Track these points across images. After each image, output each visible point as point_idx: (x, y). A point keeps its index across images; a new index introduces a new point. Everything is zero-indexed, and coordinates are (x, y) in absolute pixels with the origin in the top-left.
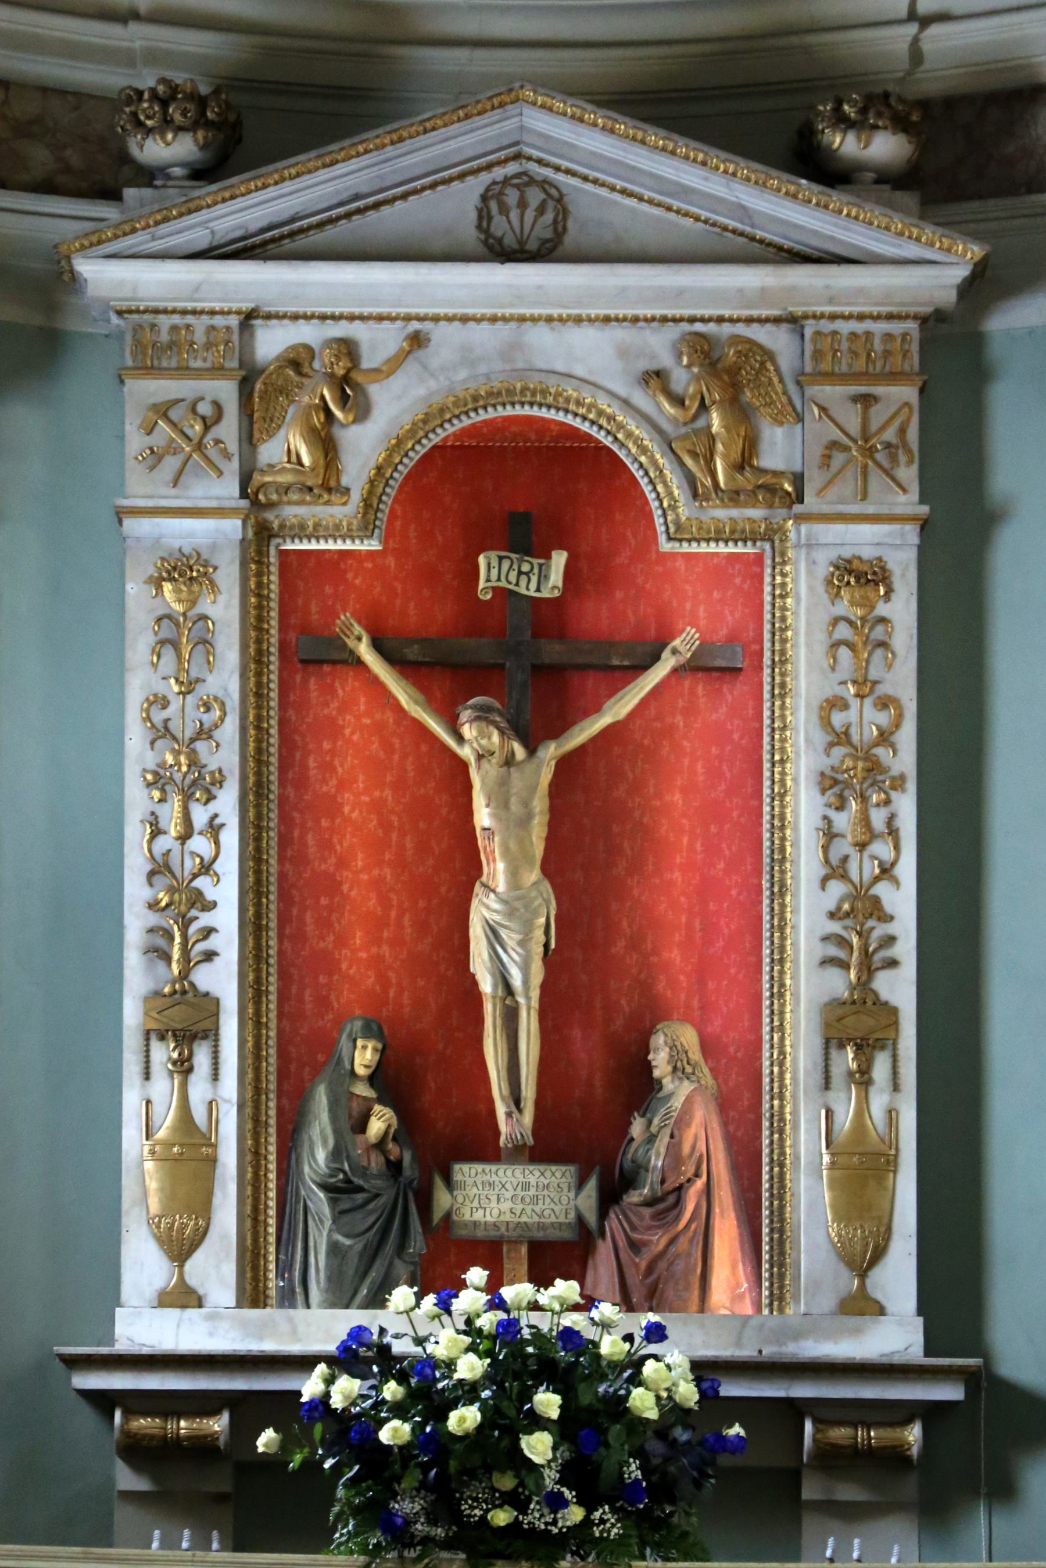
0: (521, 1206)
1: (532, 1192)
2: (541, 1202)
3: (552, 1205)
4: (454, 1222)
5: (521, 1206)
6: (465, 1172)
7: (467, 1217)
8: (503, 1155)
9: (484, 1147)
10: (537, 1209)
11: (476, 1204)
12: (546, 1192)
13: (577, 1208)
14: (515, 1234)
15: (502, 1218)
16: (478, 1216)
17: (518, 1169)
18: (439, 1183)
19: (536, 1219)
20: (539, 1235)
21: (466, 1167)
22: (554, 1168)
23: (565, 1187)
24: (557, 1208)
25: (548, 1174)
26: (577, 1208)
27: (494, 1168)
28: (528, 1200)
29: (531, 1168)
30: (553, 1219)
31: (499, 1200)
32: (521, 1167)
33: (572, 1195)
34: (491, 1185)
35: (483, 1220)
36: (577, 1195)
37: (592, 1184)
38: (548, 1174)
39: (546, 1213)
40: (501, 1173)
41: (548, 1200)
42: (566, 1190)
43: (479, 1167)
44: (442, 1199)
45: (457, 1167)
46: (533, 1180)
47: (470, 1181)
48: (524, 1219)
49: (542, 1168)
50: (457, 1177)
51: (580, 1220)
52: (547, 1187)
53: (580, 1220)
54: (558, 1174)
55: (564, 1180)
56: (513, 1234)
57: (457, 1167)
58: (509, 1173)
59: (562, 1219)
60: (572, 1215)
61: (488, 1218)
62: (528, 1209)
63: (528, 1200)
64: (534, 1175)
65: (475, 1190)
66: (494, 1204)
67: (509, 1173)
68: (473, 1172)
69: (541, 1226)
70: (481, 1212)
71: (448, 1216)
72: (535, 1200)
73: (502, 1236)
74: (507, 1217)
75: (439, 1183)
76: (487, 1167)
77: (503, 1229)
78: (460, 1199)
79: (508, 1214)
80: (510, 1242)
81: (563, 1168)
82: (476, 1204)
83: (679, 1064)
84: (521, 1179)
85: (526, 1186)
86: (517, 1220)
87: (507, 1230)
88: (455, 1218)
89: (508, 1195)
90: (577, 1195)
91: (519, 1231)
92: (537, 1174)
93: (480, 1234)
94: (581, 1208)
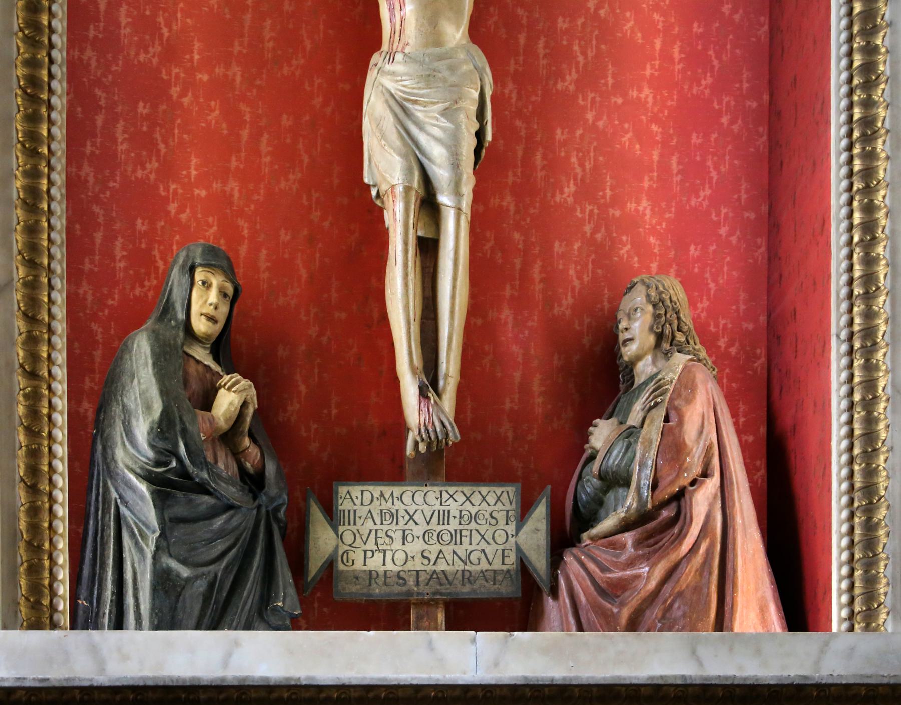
0: (438, 547)
1: (454, 525)
2: (465, 541)
3: (483, 545)
4: (337, 571)
5: (438, 547)
6: (355, 497)
7: (359, 566)
8: (409, 468)
9: (382, 457)
10: (461, 551)
11: (371, 545)
12: (473, 526)
13: (519, 550)
14: (427, 590)
15: (410, 566)
16: (375, 563)
17: (433, 492)
18: (317, 514)
19: (459, 566)
20: (465, 591)
21: (356, 491)
22: (484, 490)
23: (501, 517)
24: (489, 550)
25: (477, 499)
26: (519, 550)
27: (397, 491)
28: (447, 538)
29: (452, 490)
30: (484, 566)
31: (404, 538)
32: (437, 489)
33: (511, 529)
34: (394, 517)
35: (382, 569)
36: (518, 530)
37: (540, 511)
38: (477, 499)
39: (473, 558)
40: (407, 498)
41: (476, 538)
42: (502, 522)
43: (376, 490)
44: (323, 540)
45: (343, 490)
46: (454, 508)
47: (363, 511)
48: (442, 566)
49: (467, 490)
50: (345, 505)
51: (523, 567)
52: (473, 518)
53: (523, 567)
54: (491, 499)
55: (499, 506)
56: (426, 591)
57: (343, 490)
58: (419, 498)
59: (497, 565)
60: (511, 559)
61: (390, 566)
62: (448, 551)
63: (447, 538)
64: (456, 500)
65: (370, 524)
66: (397, 545)
67: (419, 498)
68: (367, 496)
69: (467, 577)
70: (379, 557)
71: (330, 565)
72: (457, 537)
73: (410, 593)
74: (417, 565)
75: (317, 514)
76: (387, 490)
77: (411, 582)
78: (348, 538)
79: (419, 558)
80: (422, 604)
81: (498, 491)
82: (371, 545)
83: (668, 330)
84: (438, 507)
85: (444, 517)
86: (430, 568)
87: (418, 584)
88: (341, 567)
89: (419, 531)
90: (518, 530)
91: (434, 586)
92: (461, 498)
93: (377, 591)
94: (524, 548)
